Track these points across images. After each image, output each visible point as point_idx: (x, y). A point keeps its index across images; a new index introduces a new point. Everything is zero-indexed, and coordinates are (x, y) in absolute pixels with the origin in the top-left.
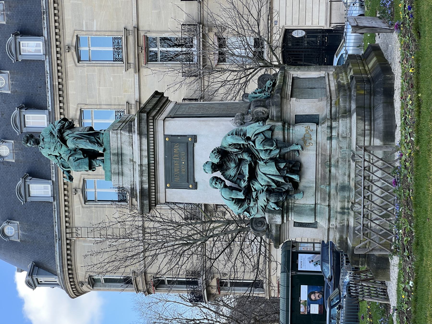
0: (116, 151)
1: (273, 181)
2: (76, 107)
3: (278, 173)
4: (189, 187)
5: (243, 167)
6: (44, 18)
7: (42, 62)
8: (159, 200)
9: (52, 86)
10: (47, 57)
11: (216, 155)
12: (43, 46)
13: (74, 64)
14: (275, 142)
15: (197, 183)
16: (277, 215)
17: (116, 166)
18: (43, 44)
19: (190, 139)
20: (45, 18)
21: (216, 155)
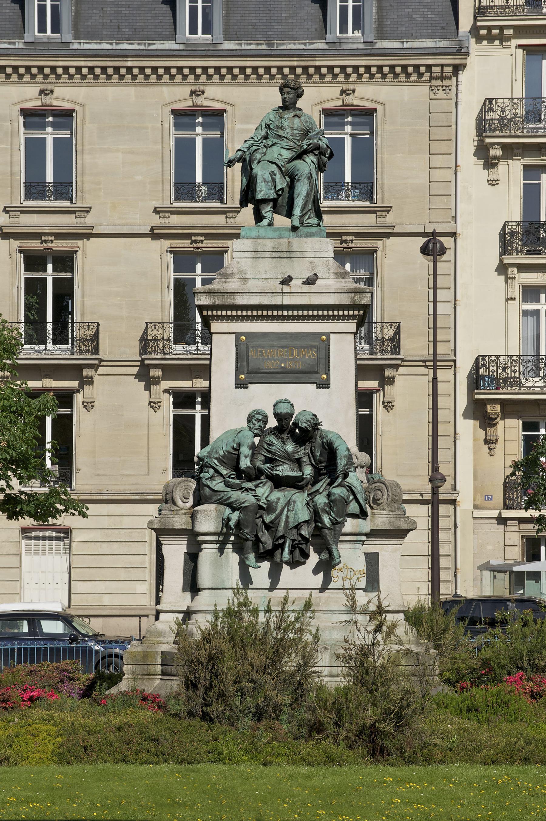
0: (295, 247)
2: (80, 101)
3: (291, 525)
4: (240, 374)
5: (287, 466)
6: (261, 44)
7: (172, 36)
9: (124, 55)
10: (181, 47)
11: (312, 421)
12: (203, 39)
13: (168, 101)
15: (247, 388)
18: (207, 40)
19: (325, 376)
20: (259, 47)
21: (312, 421)
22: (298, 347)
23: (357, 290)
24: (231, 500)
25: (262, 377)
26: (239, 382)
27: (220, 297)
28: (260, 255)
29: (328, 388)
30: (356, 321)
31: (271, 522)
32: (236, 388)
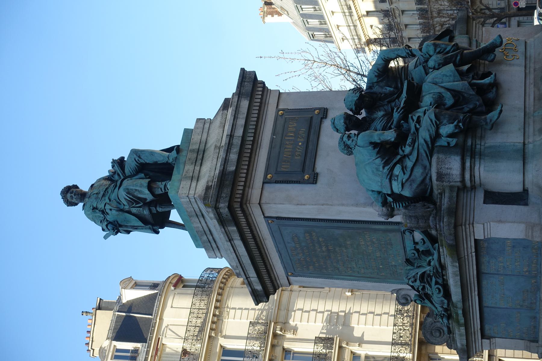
1: (448, 89)
4: (304, 179)
8: (249, 199)
16: (453, 157)
24: (428, 139)
26: (311, 180)
28: (196, 174)
31: (454, 96)
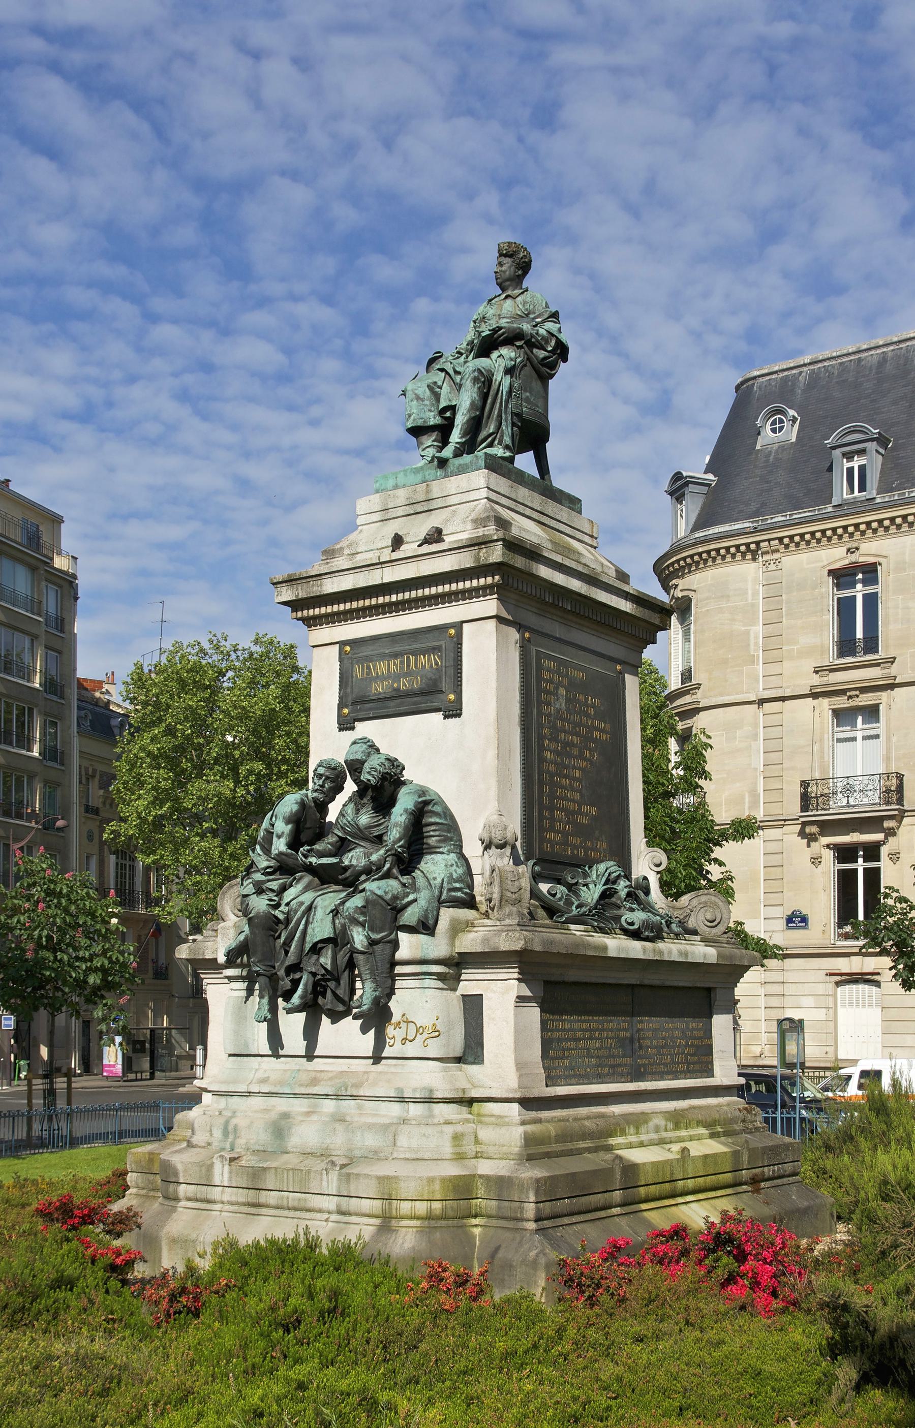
5: (362, 849)
14: (383, 938)
17: (402, 501)
19: (452, 697)
22: (415, 653)
23: (481, 540)
25: (371, 709)
27: (305, 586)
28: (392, 513)
29: (459, 715)
30: (496, 596)
32: (341, 730)
